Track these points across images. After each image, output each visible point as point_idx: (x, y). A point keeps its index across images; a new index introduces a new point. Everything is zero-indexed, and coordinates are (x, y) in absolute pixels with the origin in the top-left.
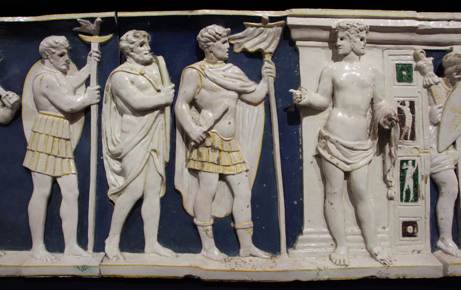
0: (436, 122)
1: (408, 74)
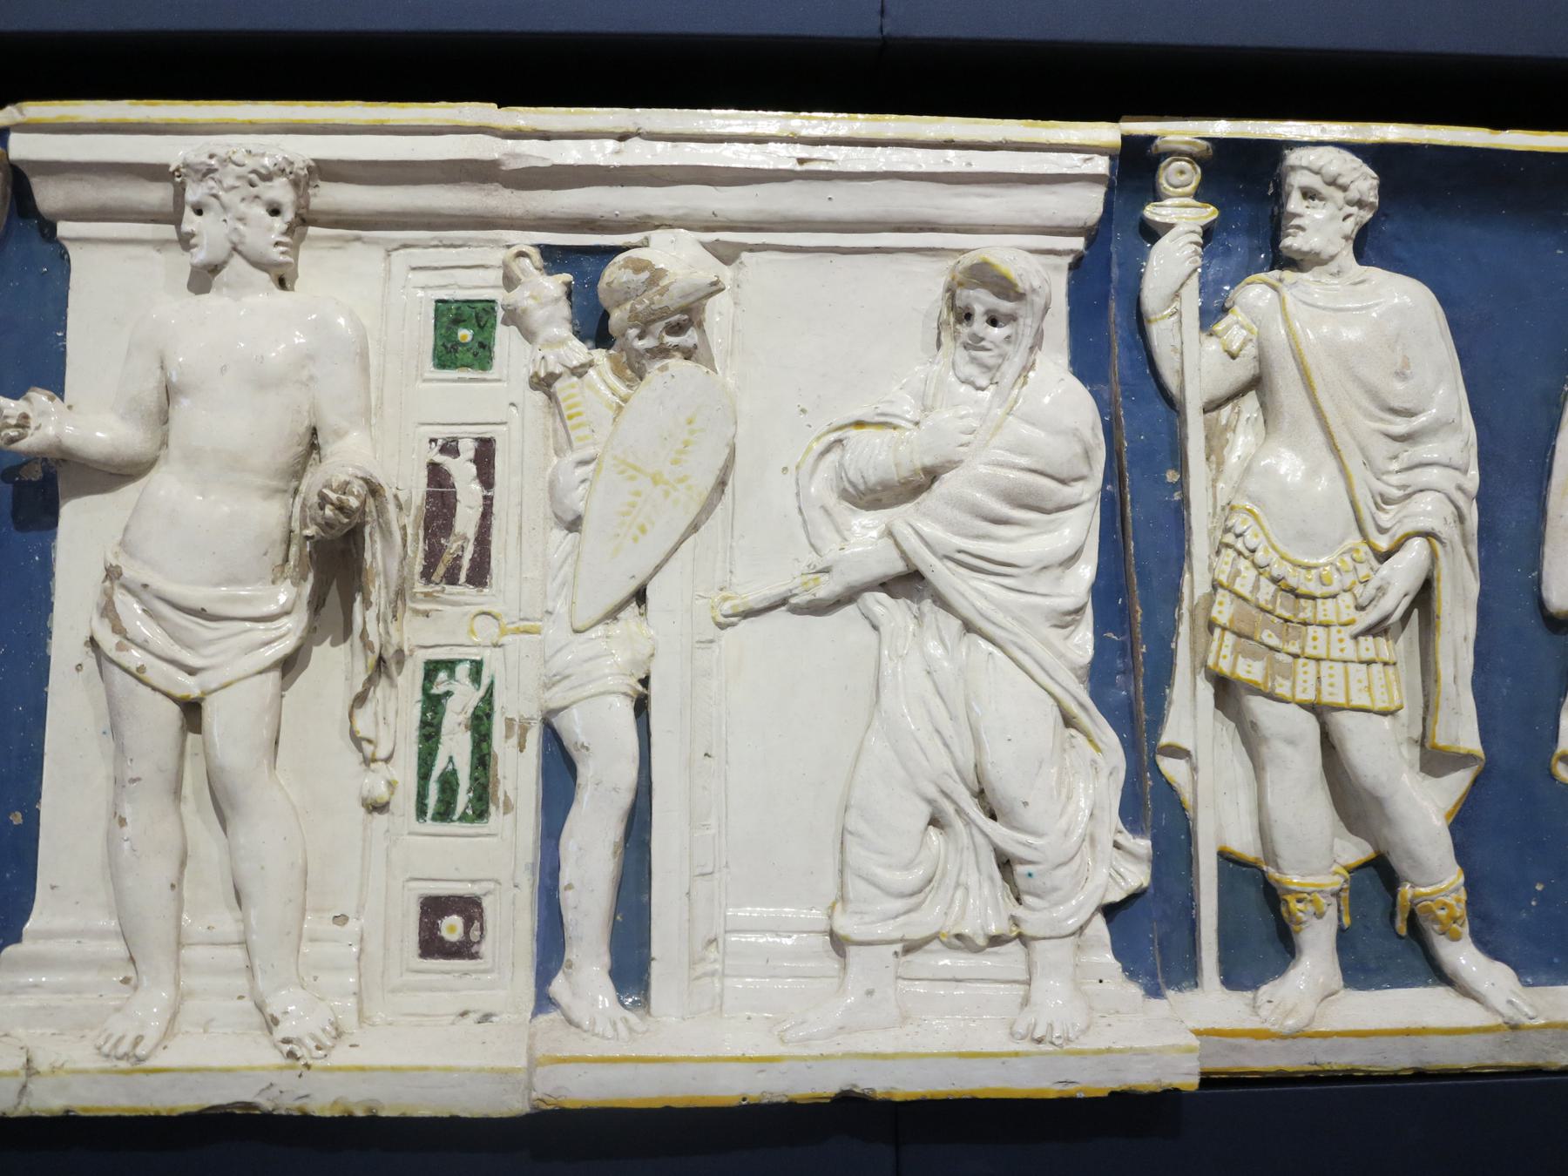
0: (569, 517)
1: (480, 339)
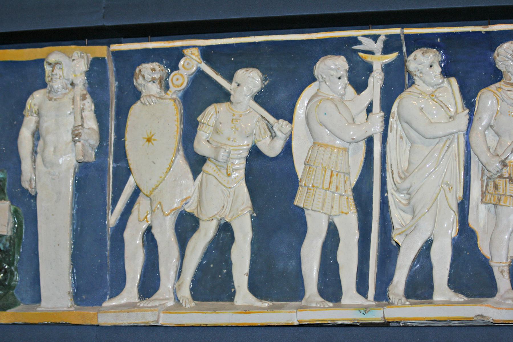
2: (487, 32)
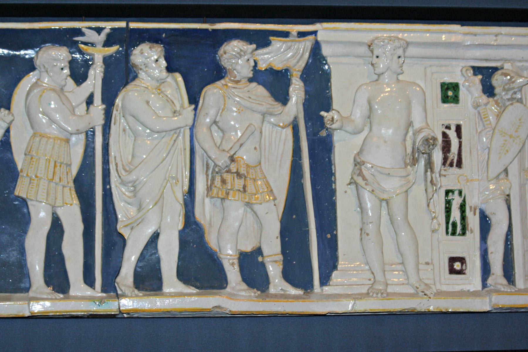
1: (455, 94)
2: (214, 30)
